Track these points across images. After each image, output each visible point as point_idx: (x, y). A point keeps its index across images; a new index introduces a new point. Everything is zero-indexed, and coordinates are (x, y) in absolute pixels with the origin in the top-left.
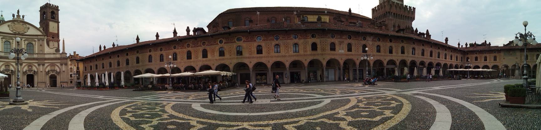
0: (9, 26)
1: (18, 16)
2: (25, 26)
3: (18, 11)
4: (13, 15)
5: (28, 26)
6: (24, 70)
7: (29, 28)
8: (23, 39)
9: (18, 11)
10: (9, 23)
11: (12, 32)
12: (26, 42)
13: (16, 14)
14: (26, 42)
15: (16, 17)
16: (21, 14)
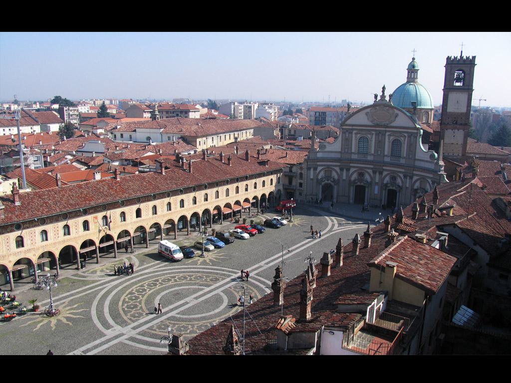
0: (367, 114)
1: (383, 96)
2: (391, 111)
3: (384, 88)
4: (376, 96)
5: (396, 111)
6: (385, 182)
7: (397, 116)
8: (387, 134)
9: (384, 88)
10: (368, 110)
11: (370, 124)
12: (392, 138)
13: (380, 94)
14: (392, 138)
15: (379, 98)
16: (387, 94)
